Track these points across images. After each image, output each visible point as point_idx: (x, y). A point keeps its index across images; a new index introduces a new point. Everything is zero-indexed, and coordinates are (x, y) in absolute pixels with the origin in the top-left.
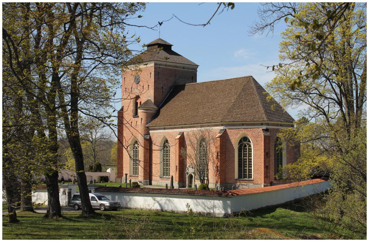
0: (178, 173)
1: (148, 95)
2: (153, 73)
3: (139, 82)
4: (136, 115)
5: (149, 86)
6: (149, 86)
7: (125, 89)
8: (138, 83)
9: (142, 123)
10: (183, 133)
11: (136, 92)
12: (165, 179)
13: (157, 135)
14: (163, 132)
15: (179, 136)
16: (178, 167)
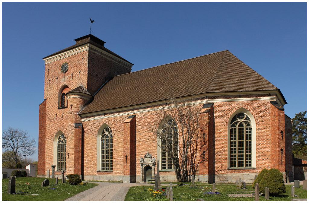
0: (129, 164)
1: (80, 79)
2: (86, 58)
3: (67, 70)
4: (62, 106)
5: (80, 72)
6: (80, 72)
7: (49, 81)
8: (66, 72)
9: (73, 110)
10: (135, 116)
11: (63, 81)
12: (106, 173)
13: (93, 123)
14: (102, 119)
15: (129, 120)
16: (129, 158)
